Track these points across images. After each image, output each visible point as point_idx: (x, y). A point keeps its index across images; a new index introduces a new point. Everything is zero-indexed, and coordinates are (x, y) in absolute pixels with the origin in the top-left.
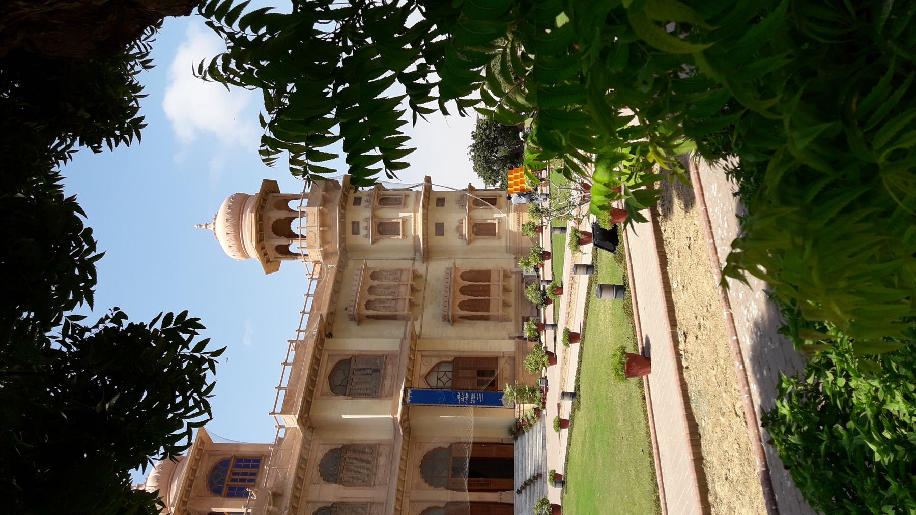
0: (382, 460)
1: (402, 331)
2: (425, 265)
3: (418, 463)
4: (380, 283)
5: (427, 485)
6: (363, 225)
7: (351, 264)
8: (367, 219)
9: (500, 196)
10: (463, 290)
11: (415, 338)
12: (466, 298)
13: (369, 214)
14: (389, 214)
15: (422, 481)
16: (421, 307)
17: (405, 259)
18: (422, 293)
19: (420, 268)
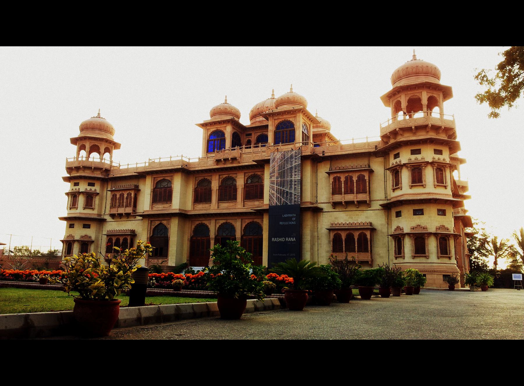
0: (257, 203)
1: (325, 201)
2: (380, 207)
3: (255, 220)
4: (355, 181)
5: (244, 226)
6: (398, 160)
7: (380, 159)
8: (400, 161)
9: (427, 257)
10: (350, 237)
11: (317, 211)
12: (344, 238)
13: (403, 162)
14: (406, 176)
15: (246, 224)
16: (344, 210)
17: (386, 193)
18: (355, 209)
19: (376, 205)
